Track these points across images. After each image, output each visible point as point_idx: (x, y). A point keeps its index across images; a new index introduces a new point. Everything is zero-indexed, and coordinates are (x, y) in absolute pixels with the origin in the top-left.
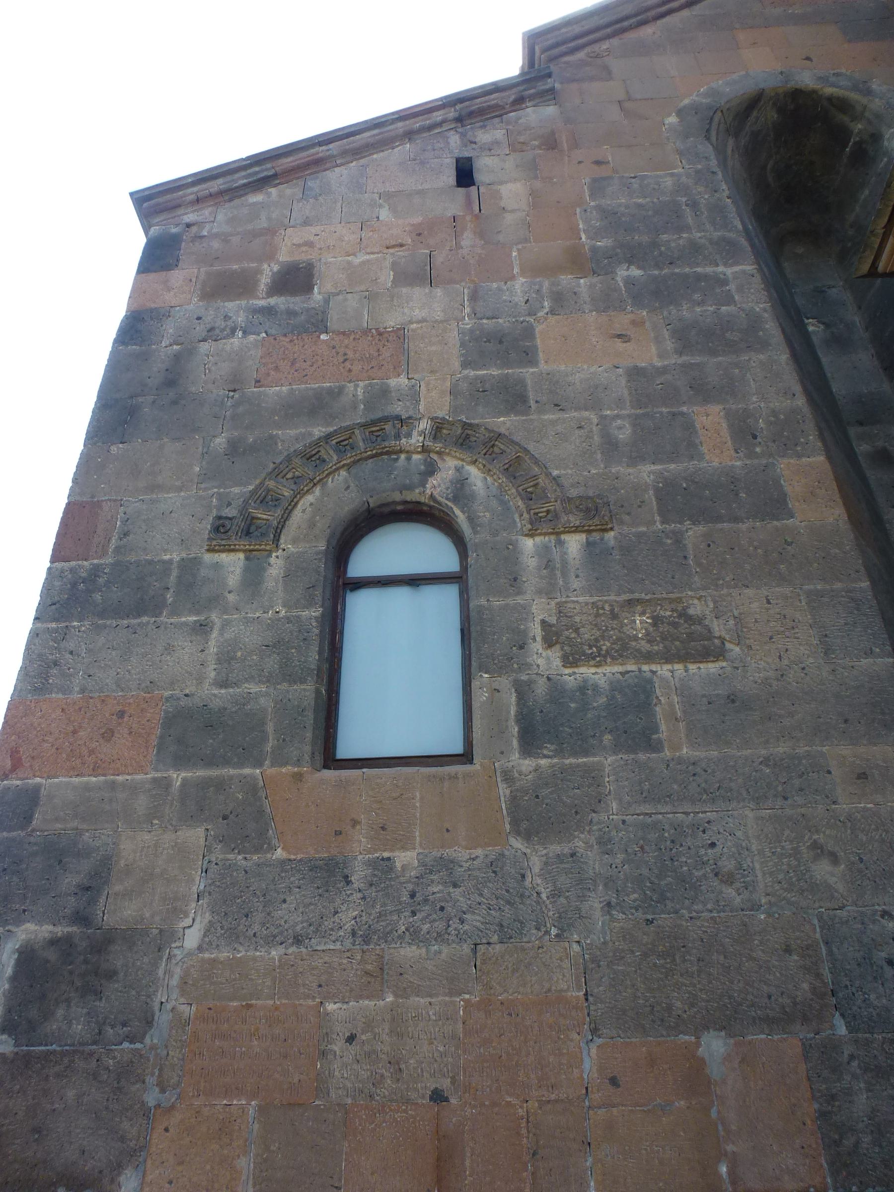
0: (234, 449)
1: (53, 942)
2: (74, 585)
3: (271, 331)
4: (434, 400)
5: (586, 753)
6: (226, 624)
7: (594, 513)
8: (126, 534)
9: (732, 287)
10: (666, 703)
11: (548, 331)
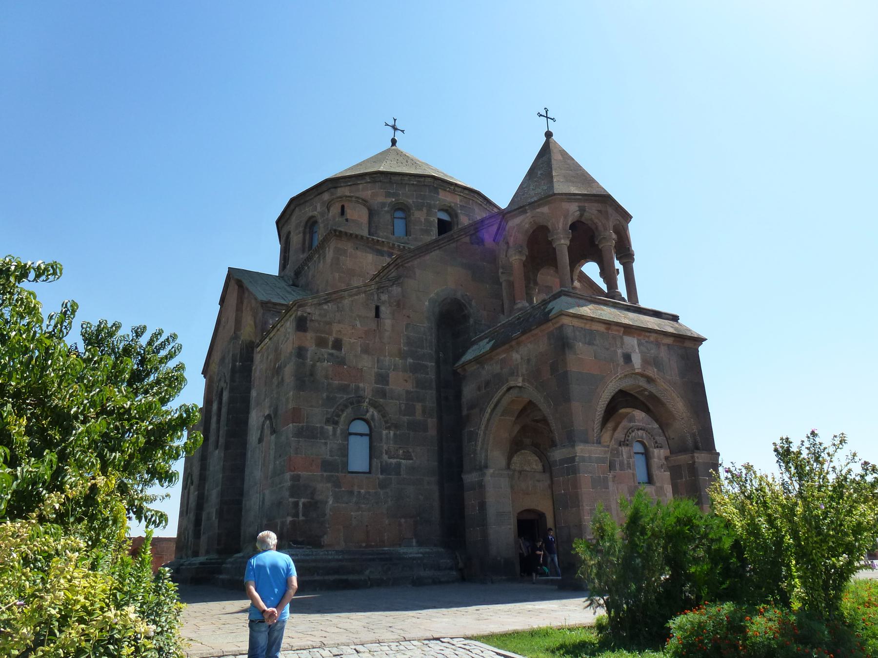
7: (396, 426)
11: (392, 375)
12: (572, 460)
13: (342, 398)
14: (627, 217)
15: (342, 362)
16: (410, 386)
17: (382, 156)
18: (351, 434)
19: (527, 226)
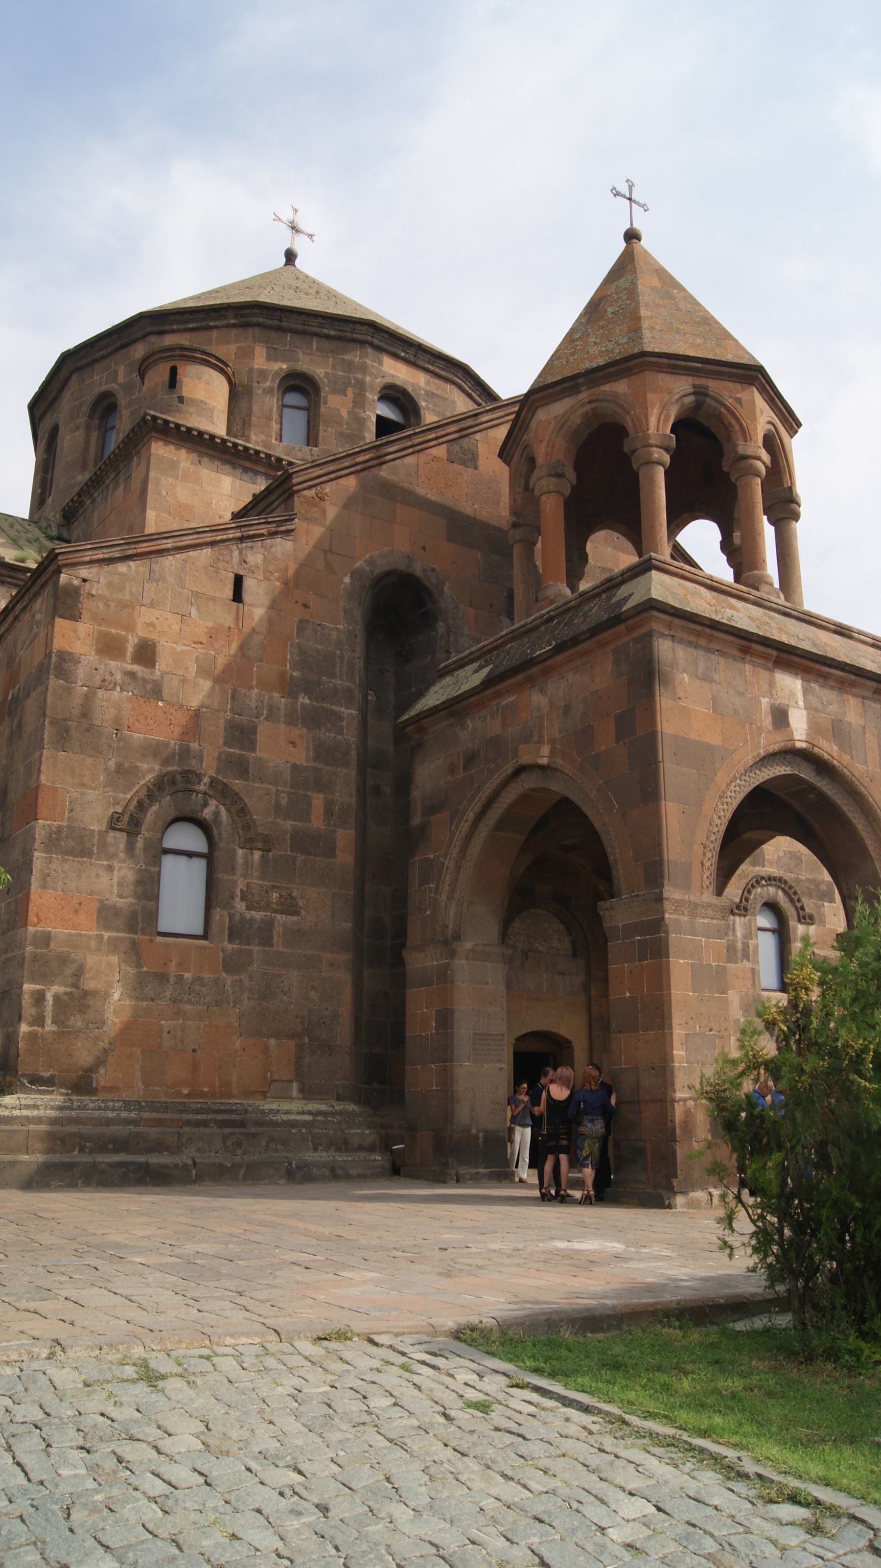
0: (120, 770)
1: (66, 994)
2: (51, 835)
3: (135, 692)
5: (249, 944)
6: (120, 868)
8: (72, 810)
9: (344, 723)
10: (278, 930)
11: (264, 730)
12: (657, 926)
13: (150, 770)
14: (792, 423)
15: (155, 692)
16: (301, 756)
17: (267, 279)
18: (167, 851)
19: (578, 421)
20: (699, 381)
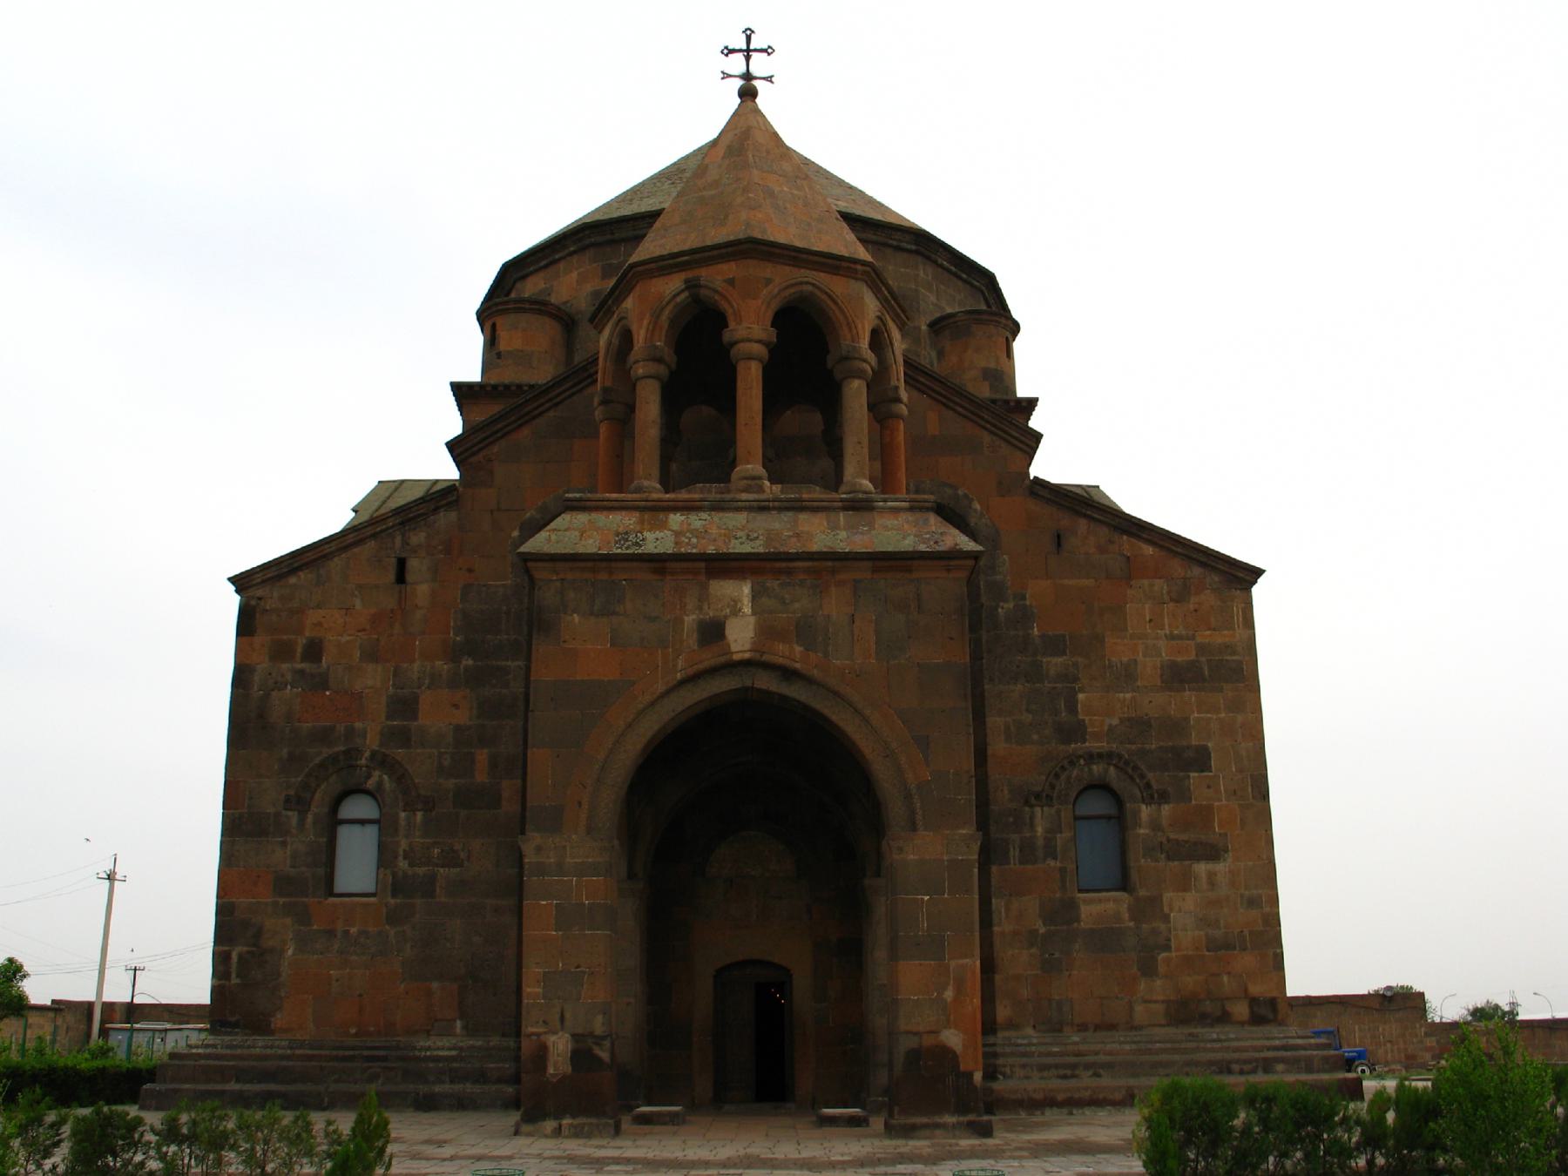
4: (372, 742)
15: (322, 682)
16: (463, 717)
20: (690, 274)
